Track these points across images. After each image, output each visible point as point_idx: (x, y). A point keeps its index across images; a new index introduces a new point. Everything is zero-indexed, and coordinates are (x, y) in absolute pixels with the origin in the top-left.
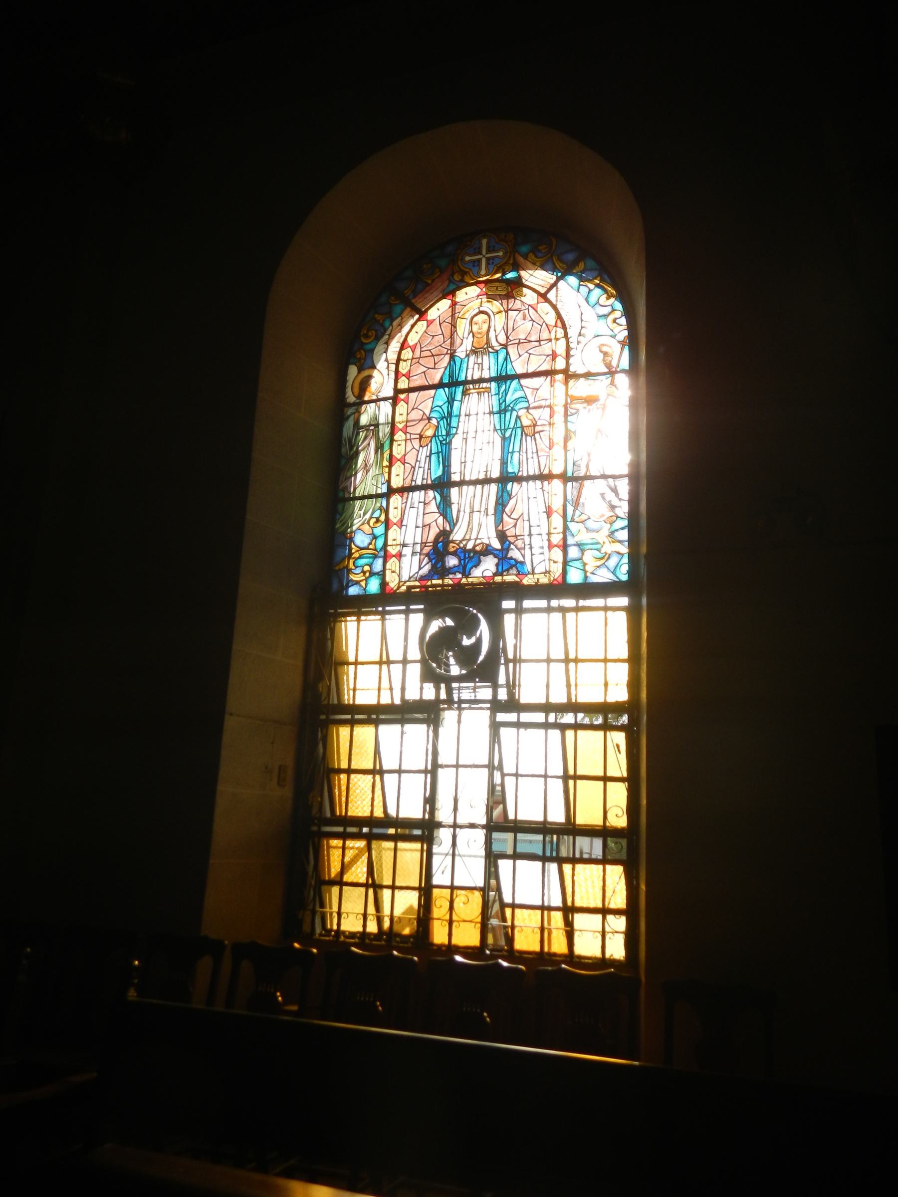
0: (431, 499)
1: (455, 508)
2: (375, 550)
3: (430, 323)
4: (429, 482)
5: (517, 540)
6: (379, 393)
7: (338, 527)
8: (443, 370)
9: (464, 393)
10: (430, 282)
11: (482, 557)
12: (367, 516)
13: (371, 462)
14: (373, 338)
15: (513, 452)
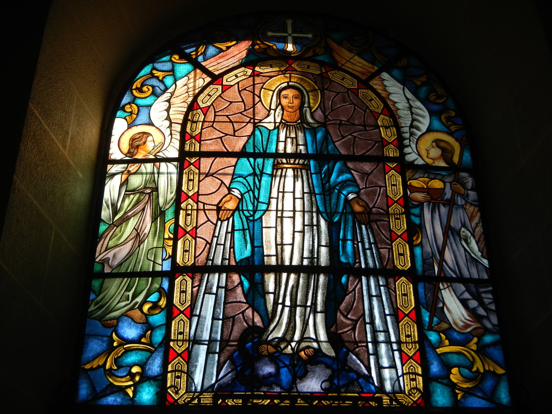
0: (236, 284)
2: (151, 344)
3: (225, 88)
4: (233, 263)
5: (358, 347)
6: (158, 152)
7: (93, 311)
8: (246, 138)
9: (275, 167)
11: (309, 366)
12: (139, 299)
13: (146, 231)
15: (345, 240)
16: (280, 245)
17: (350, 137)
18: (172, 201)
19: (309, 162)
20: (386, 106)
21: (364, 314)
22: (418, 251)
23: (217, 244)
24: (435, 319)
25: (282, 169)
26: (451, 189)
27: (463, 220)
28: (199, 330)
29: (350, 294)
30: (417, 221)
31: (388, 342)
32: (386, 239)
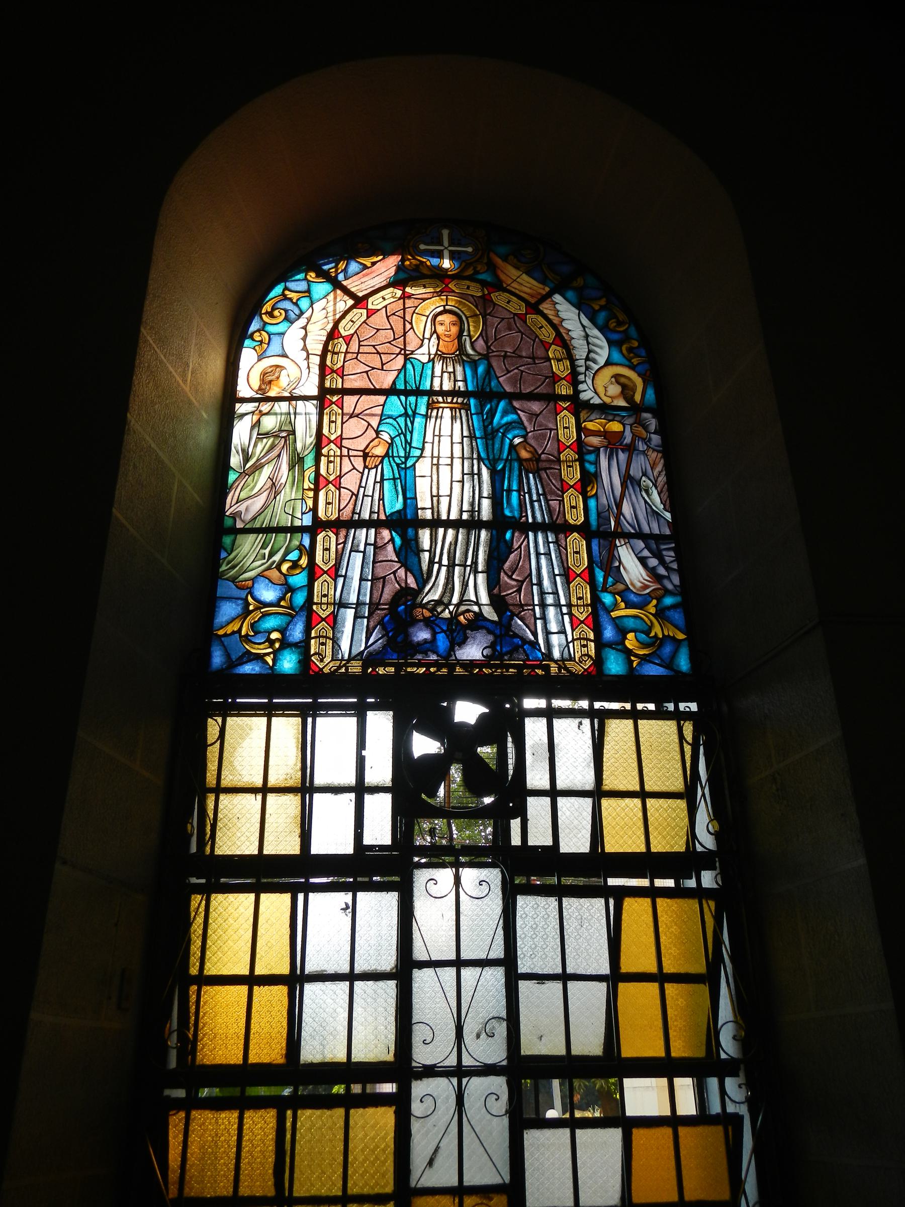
2: (291, 607)
3: (371, 313)
4: (383, 517)
5: (524, 610)
8: (396, 373)
9: (430, 406)
12: (277, 558)
15: (509, 491)
16: (436, 497)
17: (516, 371)
18: (312, 446)
19: (469, 400)
20: (559, 334)
21: (530, 574)
22: (592, 503)
23: (364, 495)
24: (610, 580)
25: (438, 409)
26: (631, 432)
27: (644, 468)
28: (345, 591)
29: (516, 552)
30: (591, 469)
31: (558, 605)
32: (556, 490)
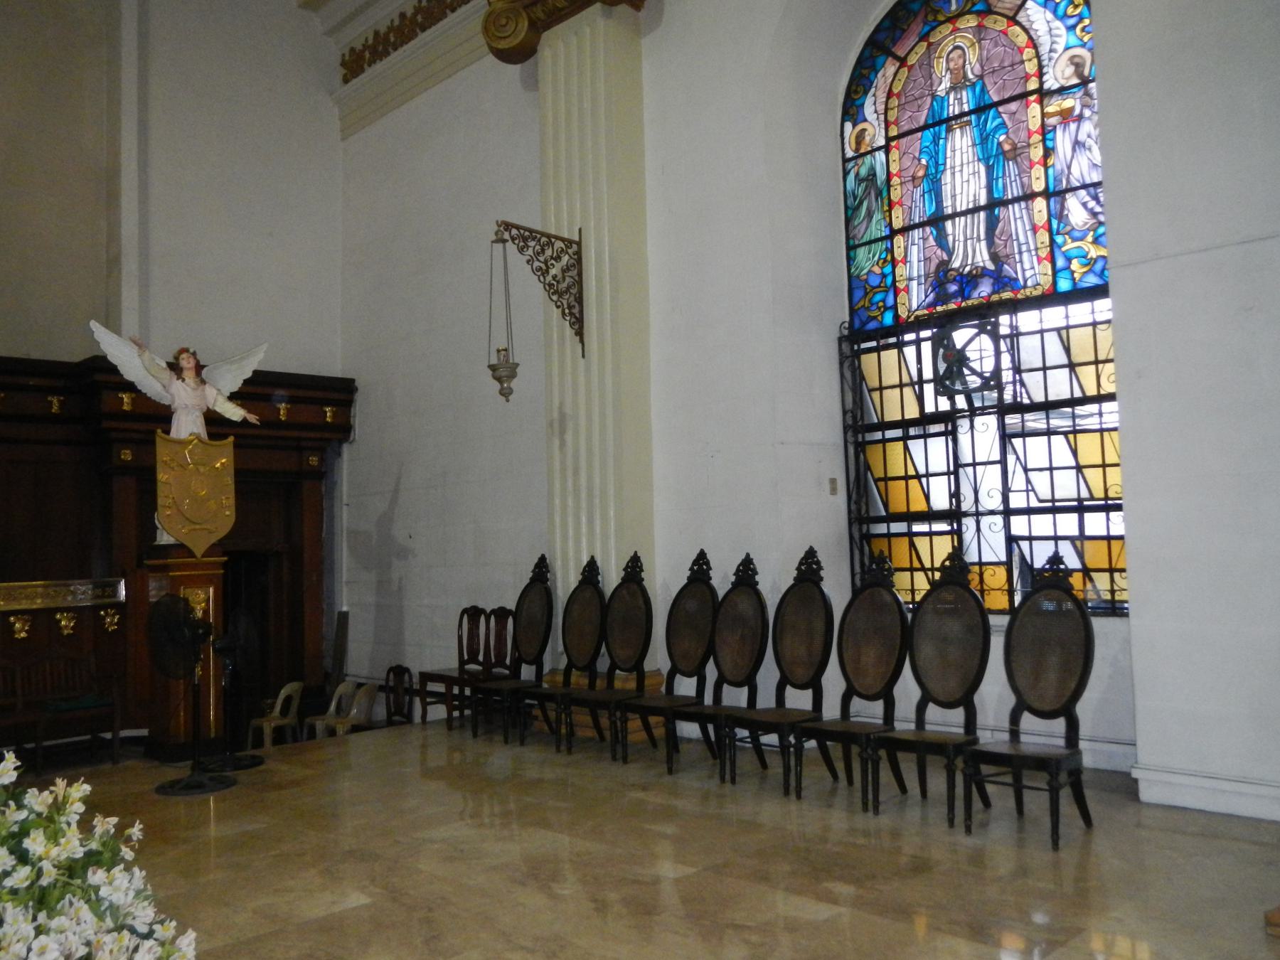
1: (950, 239)
2: (886, 287)
3: (911, 68)
4: (925, 219)
10: (905, 27)
12: (876, 258)
13: (873, 209)
14: (861, 94)
15: (997, 179)
20: (1030, 38)
21: (1011, 235)
22: (1051, 171)
30: (1050, 144)
31: (1029, 251)
